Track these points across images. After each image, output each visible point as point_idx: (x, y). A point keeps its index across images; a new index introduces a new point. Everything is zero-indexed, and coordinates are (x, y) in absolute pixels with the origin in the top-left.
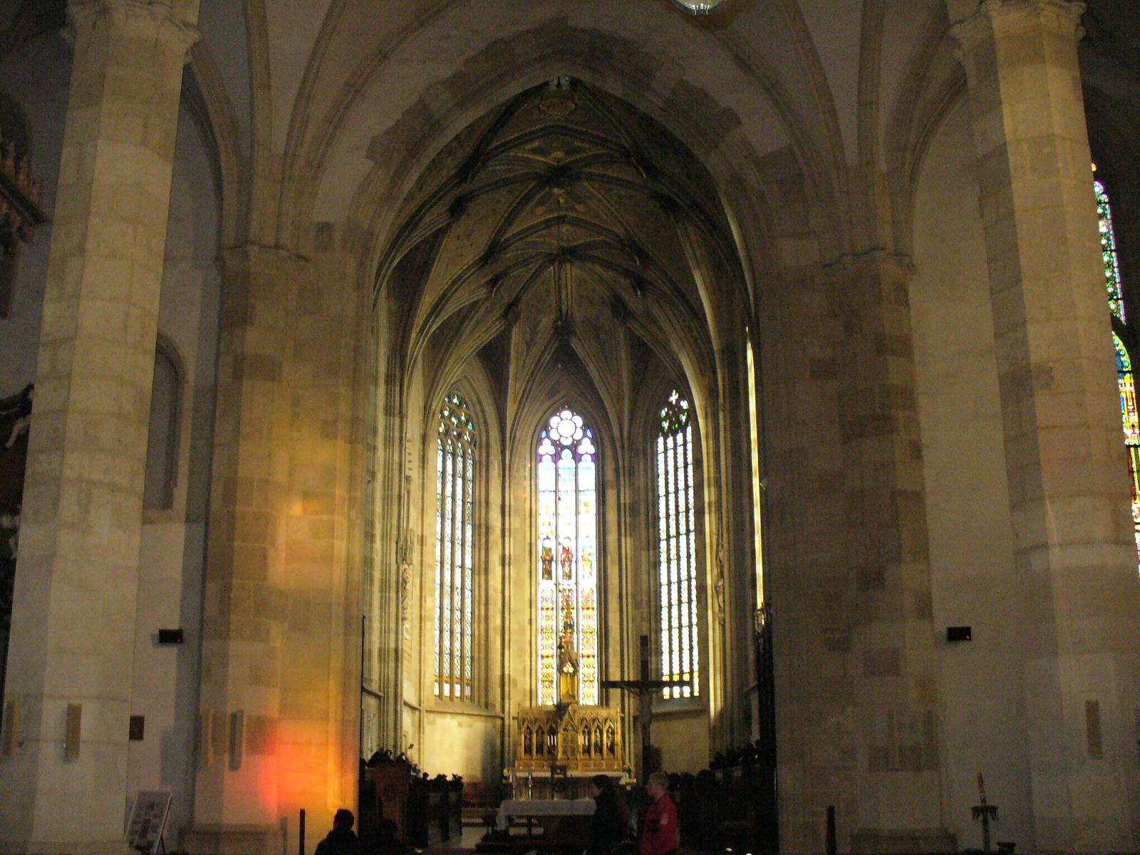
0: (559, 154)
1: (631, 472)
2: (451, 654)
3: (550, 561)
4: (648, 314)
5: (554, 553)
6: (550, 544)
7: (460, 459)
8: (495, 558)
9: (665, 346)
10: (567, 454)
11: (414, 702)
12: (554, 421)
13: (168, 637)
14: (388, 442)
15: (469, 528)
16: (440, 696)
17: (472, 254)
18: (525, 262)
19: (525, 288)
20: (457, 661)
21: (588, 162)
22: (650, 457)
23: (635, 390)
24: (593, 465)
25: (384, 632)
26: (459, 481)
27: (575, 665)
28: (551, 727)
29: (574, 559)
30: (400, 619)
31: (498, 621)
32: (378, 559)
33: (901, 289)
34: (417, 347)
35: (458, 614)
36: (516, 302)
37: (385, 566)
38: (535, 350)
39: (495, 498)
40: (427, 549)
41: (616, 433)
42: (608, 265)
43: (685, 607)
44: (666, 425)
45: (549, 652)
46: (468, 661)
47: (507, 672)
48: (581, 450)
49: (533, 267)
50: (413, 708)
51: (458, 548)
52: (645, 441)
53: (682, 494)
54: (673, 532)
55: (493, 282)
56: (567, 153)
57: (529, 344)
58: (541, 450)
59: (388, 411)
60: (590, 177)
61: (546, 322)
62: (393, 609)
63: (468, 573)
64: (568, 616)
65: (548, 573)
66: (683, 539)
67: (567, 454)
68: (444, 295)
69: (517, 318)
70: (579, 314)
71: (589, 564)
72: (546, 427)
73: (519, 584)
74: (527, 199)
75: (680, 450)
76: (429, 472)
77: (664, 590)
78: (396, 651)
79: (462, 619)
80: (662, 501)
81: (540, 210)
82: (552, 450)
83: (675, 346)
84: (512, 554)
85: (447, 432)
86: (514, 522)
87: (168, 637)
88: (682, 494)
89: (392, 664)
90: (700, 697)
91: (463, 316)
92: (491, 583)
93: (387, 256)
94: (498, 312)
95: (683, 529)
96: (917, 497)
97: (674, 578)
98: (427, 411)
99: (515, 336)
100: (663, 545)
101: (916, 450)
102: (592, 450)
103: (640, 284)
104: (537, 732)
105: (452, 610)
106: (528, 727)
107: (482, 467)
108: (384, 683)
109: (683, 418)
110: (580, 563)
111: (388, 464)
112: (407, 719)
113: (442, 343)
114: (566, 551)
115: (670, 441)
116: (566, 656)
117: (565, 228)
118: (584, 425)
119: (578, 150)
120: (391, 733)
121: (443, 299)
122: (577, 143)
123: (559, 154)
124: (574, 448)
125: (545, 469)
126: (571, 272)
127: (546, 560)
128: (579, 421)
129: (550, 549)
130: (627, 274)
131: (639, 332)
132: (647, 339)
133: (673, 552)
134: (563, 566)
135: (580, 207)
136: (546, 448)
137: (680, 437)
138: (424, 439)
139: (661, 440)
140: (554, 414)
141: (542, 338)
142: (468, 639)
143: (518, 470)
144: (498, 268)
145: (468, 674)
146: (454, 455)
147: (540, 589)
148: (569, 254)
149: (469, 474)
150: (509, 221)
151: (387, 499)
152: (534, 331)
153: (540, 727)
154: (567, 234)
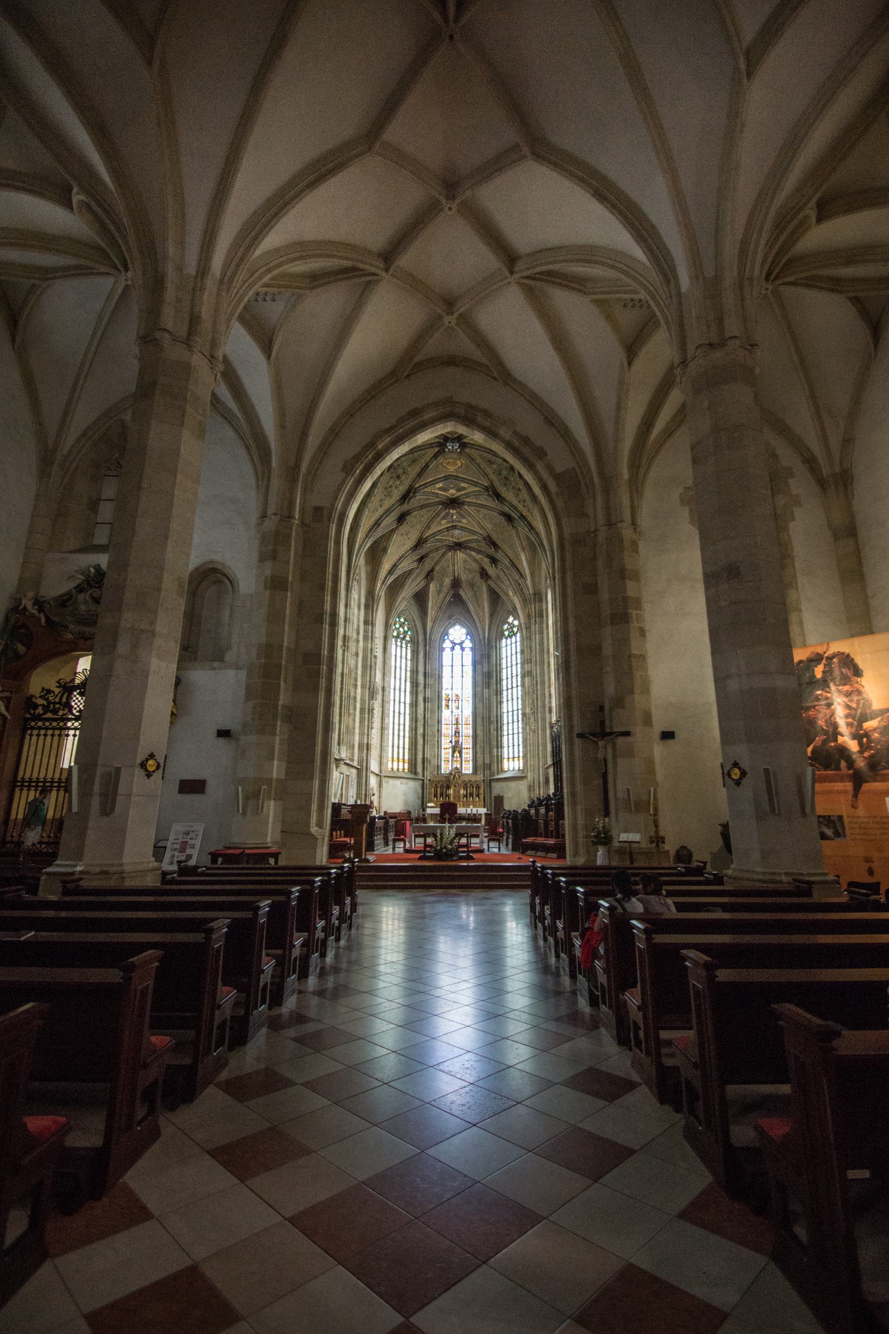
0: (452, 491)
2: (398, 747)
4: (498, 577)
6: (449, 692)
7: (404, 650)
8: (421, 699)
9: (507, 594)
10: (458, 647)
11: (377, 772)
12: (451, 631)
13: (224, 734)
14: (366, 638)
15: (408, 684)
16: (392, 769)
17: (409, 544)
18: (437, 549)
19: (437, 563)
20: (401, 750)
21: (467, 495)
22: (498, 649)
23: (492, 615)
24: (471, 653)
25: (361, 734)
26: (404, 660)
27: (460, 752)
30: (370, 728)
32: (359, 698)
33: (635, 545)
34: (381, 590)
35: (402, 727)
36: (432, 570)
37: (363, 701)
38: (442, 596)
39: (421, 669)
40: (386, 693)
41: (481, 637)
42: (479, 552)
43: (516, 724)
44: (506, 633)
45: (448, 746)
46: (407, 751)
48: (464, 645)
49: (441, 552)
50: (377, 775)
51: (402, 693)
53: (514, 667)
54: (510, 687)
55: (421, 559)
56: (458, 490)
57: (439, 592)
58: (444, 645)
59: (366, 622)
60: (469, 504)
61: (447, 581)
62: (366, 723)
63: (408, 706)
64: (457, 728)
65: (448, 706)
66: (515, 690)
67: (458, 647)
68: (395, 565)
69: (432, 579)
70: (464, 577)
72: (447, 634)
73: (432, 712)
74: (438, 514)
75: (514, 645)
76: (387, 655)
77: (505, 715)
78: (368, 744)
79: (404, 730)
80: (504, 671)
81: (444, 522)
82: (451, 645)
83: (511, 594)
85: (397, 637)
86: (430, 681)
87: (224, 734)
88: (514, 667)
89: (365, 752)
90: (523, 770)
91: (406, 575)
93: (363, 542)
94: (422, 576)
95: (515, 685)
96: (643, 657)
97: (510, 710)
98: (387, 626)
99: (432, 587)
100: (505, 693)
101: (643, 633)
102: (470, 645)
103: (494, 561)
105: (399, 724)
107: (415, 653)
108: (360, 762)
109: (515, 630)
111: (365, 650)
112: (373, 781)
113: (394, 590)
114: (457, 696)
115: (509, 640)
116: (457, 748)
117: (457, 532)
119: (463, 489)
120: (364, 788)
121: (394, 567)
122: (463, 485)
123: (452, 491)
124: (461, 644)
125: (446, 656)
126: (460, 555)
128: (464, 631)
130: (488, 556)
131: (493, 586)
132: (498, 590)
133: (510, 696)
135: (464, 521)
136: (447, 644)
137: (514, 639)
138: (386, 639)
139: (504, 640)
140: (451, 627)
141: (445, 590)
142: (407, 740)
144: (422, 551)
145: (406, 758)
146: (401, 647)
147: (443, 714)
148: (458, 546)
149: (409, 657)
150: (428, 527)
151: (364, 667)
152: (441, 585)
154: (458, 535)
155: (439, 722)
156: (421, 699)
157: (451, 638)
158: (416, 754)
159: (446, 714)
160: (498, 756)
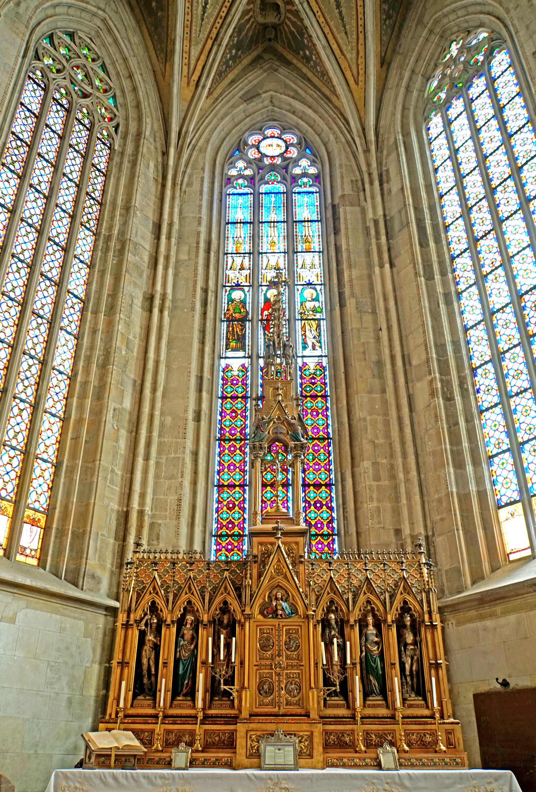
1: (383, 179)
3: (243, 320)
5: (249, 307)
8: (133, 290)
23: (384, 63)
28: (225, 608)
31: (128, 403)
52: (406, 134)
65: (241, 339)
71: (314, 324)
92: (121, 327)
106: (154, 608)
110: (299, 324)
118: (299, 143)
129: (243, 303)
134: (266, 328)
143: (189, 184)
153: (189, 608)
156: (133, 290)
157: (252, 154)
158: (88, 489)
160: (464, 498)
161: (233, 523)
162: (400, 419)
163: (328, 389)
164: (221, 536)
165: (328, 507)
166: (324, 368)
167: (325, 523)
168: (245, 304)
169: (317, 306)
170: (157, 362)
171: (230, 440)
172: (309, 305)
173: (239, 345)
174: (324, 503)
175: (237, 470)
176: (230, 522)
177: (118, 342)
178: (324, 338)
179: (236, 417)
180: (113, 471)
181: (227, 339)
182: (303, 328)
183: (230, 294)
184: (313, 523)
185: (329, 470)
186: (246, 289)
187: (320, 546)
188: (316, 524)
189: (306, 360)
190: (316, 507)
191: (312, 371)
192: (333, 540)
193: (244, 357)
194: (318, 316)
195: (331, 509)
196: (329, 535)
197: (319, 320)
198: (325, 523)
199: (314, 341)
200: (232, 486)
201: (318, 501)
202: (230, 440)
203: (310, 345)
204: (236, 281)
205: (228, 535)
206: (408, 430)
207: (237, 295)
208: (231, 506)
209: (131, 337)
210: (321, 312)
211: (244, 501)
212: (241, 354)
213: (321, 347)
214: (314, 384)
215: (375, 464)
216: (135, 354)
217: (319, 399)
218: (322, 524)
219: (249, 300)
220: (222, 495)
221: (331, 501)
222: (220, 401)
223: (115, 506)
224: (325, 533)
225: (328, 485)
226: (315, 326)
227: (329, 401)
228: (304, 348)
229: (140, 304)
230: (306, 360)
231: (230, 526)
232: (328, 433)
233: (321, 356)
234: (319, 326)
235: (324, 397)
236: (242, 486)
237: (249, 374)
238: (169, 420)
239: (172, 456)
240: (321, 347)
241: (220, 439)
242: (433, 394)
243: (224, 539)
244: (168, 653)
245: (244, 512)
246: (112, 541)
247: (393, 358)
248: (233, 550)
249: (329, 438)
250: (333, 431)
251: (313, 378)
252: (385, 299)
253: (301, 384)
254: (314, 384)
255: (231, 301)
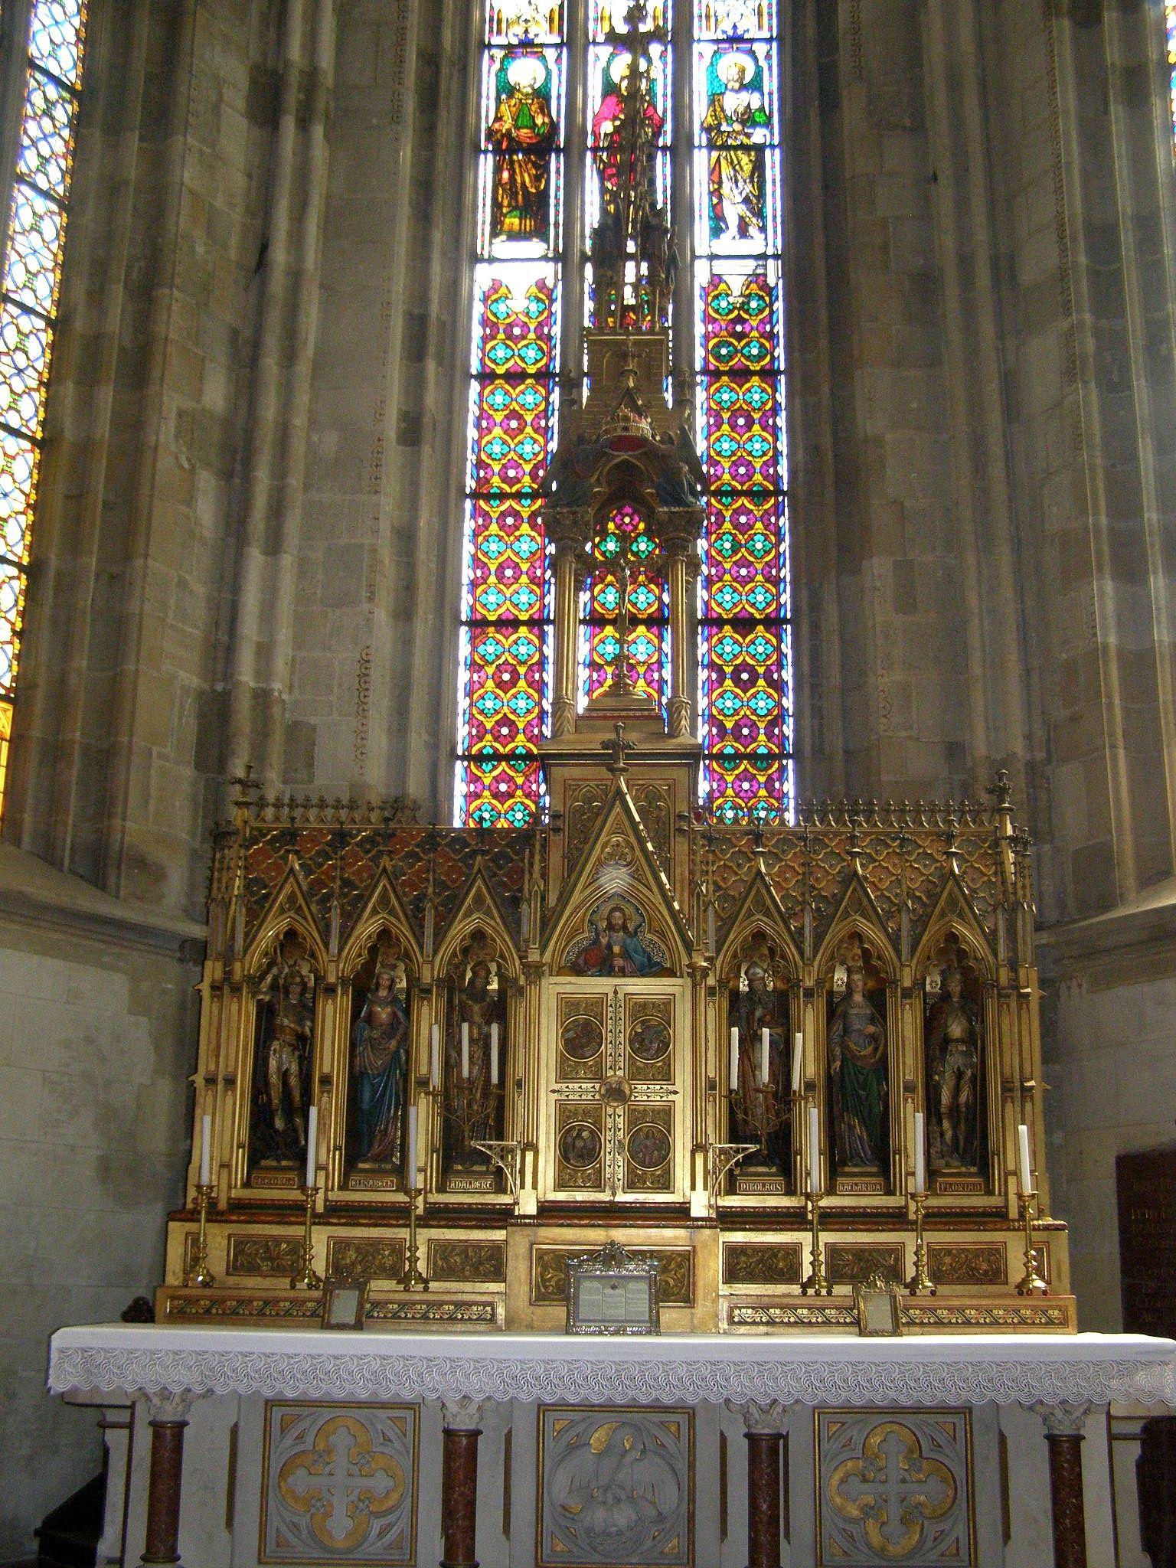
3: (542, 147)
5: (558, 108)
29: (666, 139)
47: (246, 675)
73: (351, 225)
84: (326, 60)
92: (189, 175)
104: (362, 986)
110: (701, 161)
127: (515, 146)
129: (542, 96)
147: (483, 276)
155: (431, 335)
159: (513, 273)
161: (511, 724)
162: (978, 442)
163: (780, 351)
164: (480, 759)
165: (771, 683)
166: (770, 291)
167: (762, 725)
168: (547, 98)
169: (755, 105)
170: (296, 275)
171: (502, 496)
172: (734, 103)
173: (529, 224)
174: (761, 670)
175: (524, 579)
176: (505, 721)
177: (182, 220)
178: (774, 202)
179: (520, 430)
180: (182, 584)
181: (496, 205)
182: (715, 171)
183: (503, 69)
184: (729, 725)
185: (777, 581)
186: (551, 54)
187: (746, 786)
188: (738, 726)
189: (719, 267)
190: (737, 681)
191: (736, 299)
192: (782, 769)
193: (545, 258)
194: (759, 136)
195: (779, 686)
196: (770, 757)
197: (760, 149)
198: (762, 725)
199: (742, 209)
200: (507, 624)
201: (744, 667)
202: (502, 496)
203: (733, 221)
204: (519, 30)
205: (497, 757)
206: (996, 471)
207: (525, 73)
208: (506, 677)
209: (219, 203)
210: (768, 124)
211: (541, 664)
212: (535, 247)
213: (763, 229)
214: (740, 337)
215: (904, 568)
216: (233, 253)
217: (755, 380)
218: (753, 726)
219: (558, 88)
220: (481, 649)
221: (780, 666)
222: (475, 386)
223: (190, 679)
224: (762, 750)
225: (773, 623)
226: (748, 168)
227: (782, 388)
228: (717, 231)
229: (240, 103)
230: (719, 267)
231: (505, 731)
232: (776, 479)
233: (763, 257)
234: (759, 167)
235: (769, 375)
236: (536, 623)
237: (557, 307)
238: (330, 442)
239: (344, 541)
240: (763, 229)
241: (475, 495)
242: (1071, 371)
243: (487, 767)
244: (331, 1056)
245: (542, 695)
246: (188, 772)
247: (966, 262)
248: (510, 795)
249: (778, 492)
250: (792, 472)
251: (739, 320)
252: (954, 86)
253: (707, 337)
254: (740, 337)
255: (507, 90)
